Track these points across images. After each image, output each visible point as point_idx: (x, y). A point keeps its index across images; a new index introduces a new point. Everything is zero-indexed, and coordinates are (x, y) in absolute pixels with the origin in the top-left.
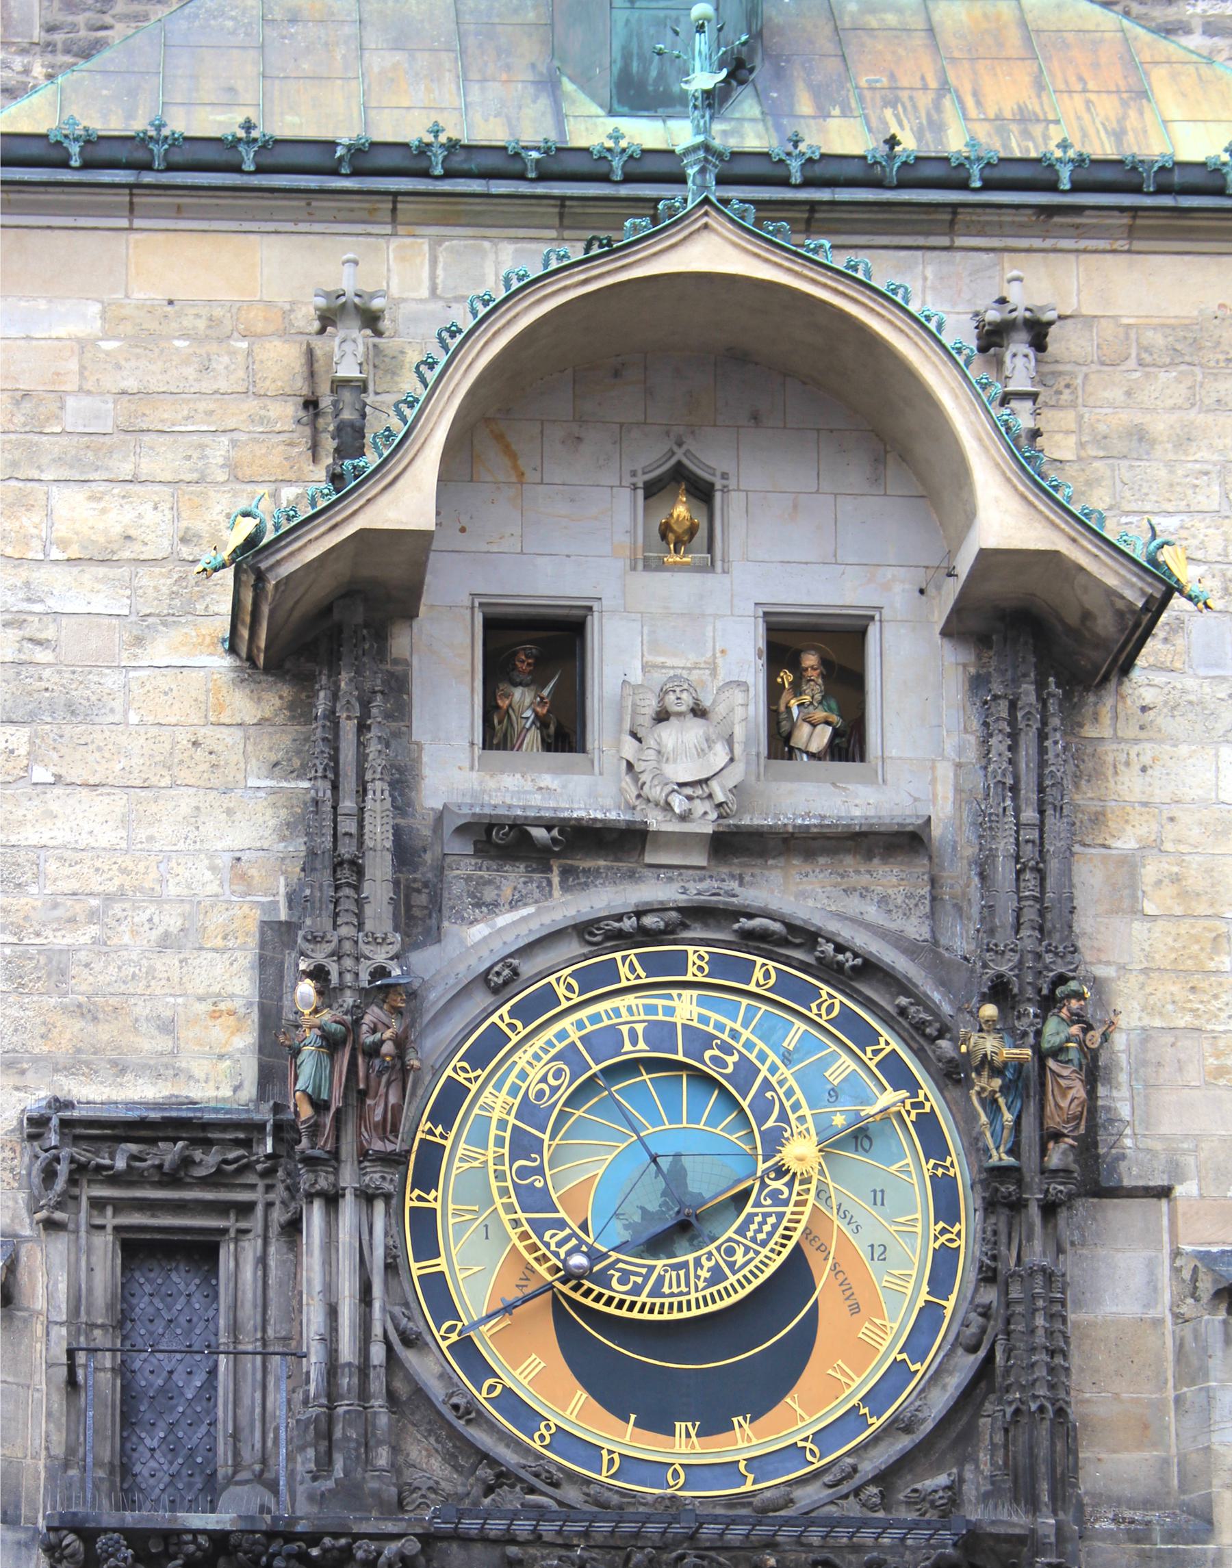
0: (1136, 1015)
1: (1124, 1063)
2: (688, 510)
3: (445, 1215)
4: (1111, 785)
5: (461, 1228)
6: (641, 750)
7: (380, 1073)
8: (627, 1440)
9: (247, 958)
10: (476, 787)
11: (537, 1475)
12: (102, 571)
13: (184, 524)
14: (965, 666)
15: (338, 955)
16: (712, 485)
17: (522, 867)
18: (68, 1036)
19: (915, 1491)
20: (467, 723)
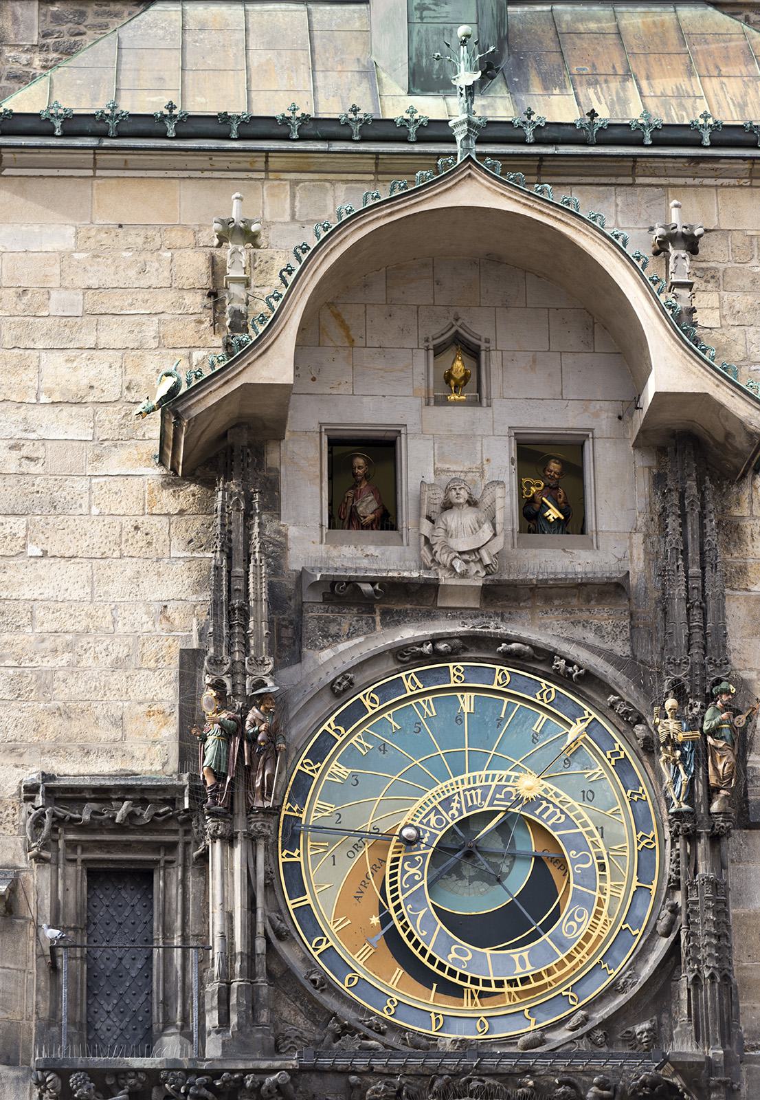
2: (463, 364)
6: (434, 529)
7: (260, 753)
8: (431, 1002)
10: (325, 555)
11: (370, 1027)
13: (128, 377)
14: (650, 468)
15: (232, 673)
16: (479, 346)
18: (51, 730)
19: (629, 1032)
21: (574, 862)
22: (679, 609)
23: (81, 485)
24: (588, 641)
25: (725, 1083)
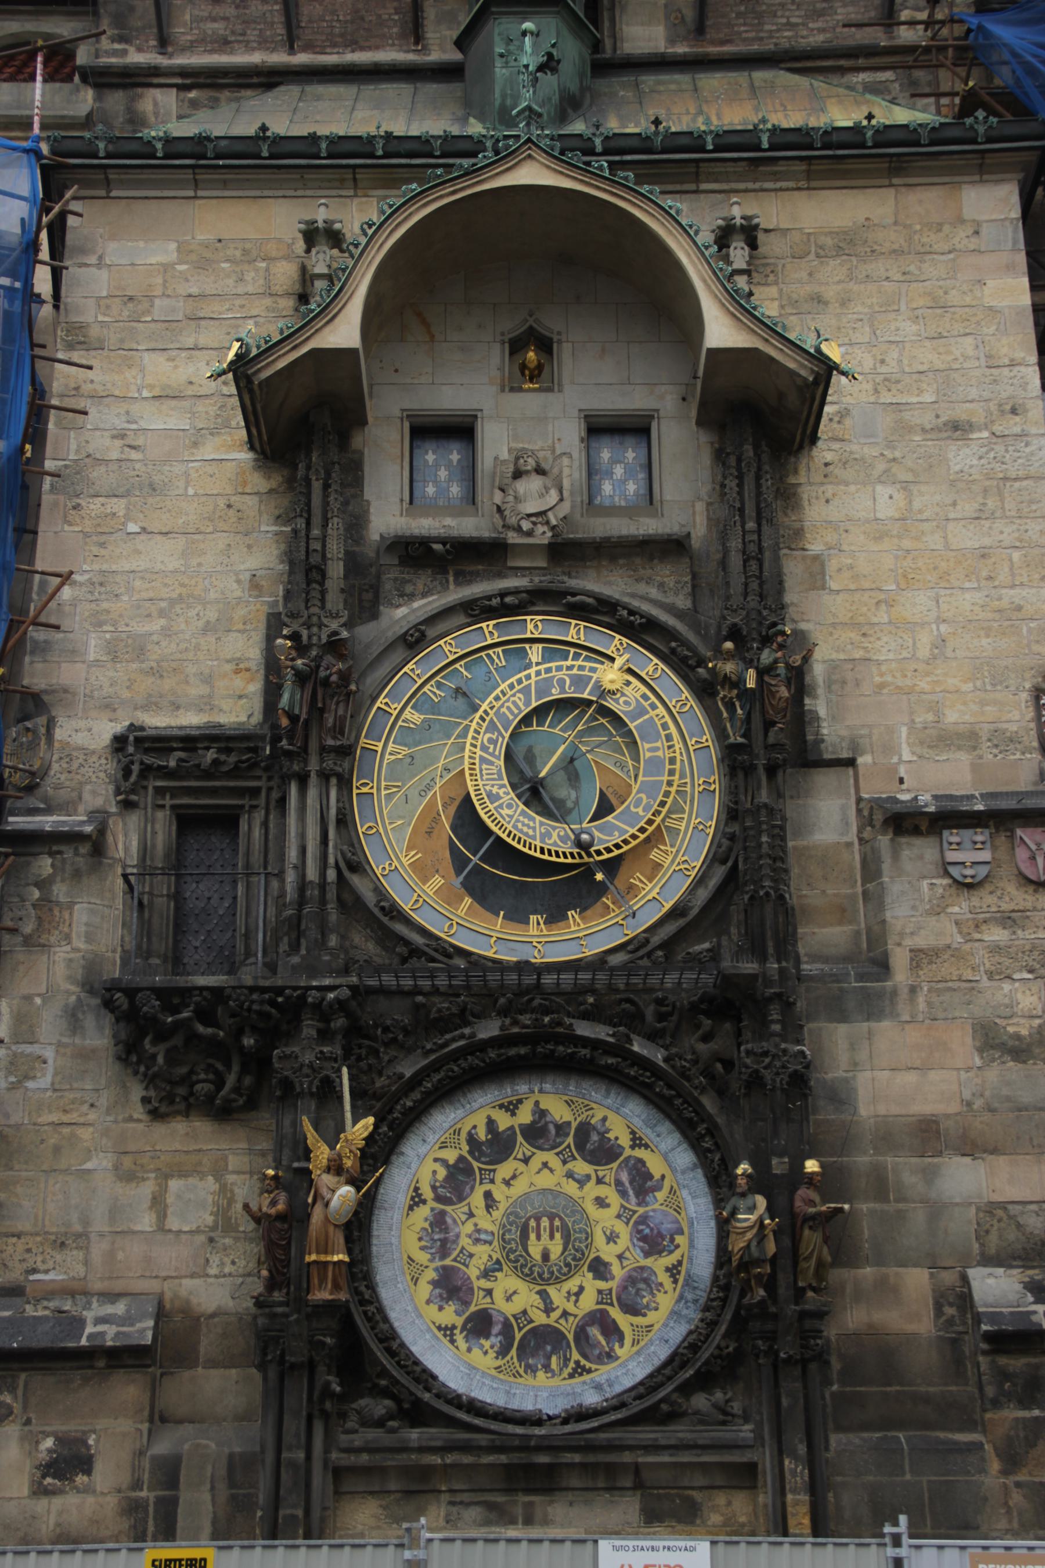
4: (807, 511)
5: (389, 797)
8: (498, 928)
9: (258, 637)
11: (436, 950)
14: (712, 443)
17: (430, 572)
20: (399, 488)
21: (563, 690)
23: (178, 469)
25: (779, 996)
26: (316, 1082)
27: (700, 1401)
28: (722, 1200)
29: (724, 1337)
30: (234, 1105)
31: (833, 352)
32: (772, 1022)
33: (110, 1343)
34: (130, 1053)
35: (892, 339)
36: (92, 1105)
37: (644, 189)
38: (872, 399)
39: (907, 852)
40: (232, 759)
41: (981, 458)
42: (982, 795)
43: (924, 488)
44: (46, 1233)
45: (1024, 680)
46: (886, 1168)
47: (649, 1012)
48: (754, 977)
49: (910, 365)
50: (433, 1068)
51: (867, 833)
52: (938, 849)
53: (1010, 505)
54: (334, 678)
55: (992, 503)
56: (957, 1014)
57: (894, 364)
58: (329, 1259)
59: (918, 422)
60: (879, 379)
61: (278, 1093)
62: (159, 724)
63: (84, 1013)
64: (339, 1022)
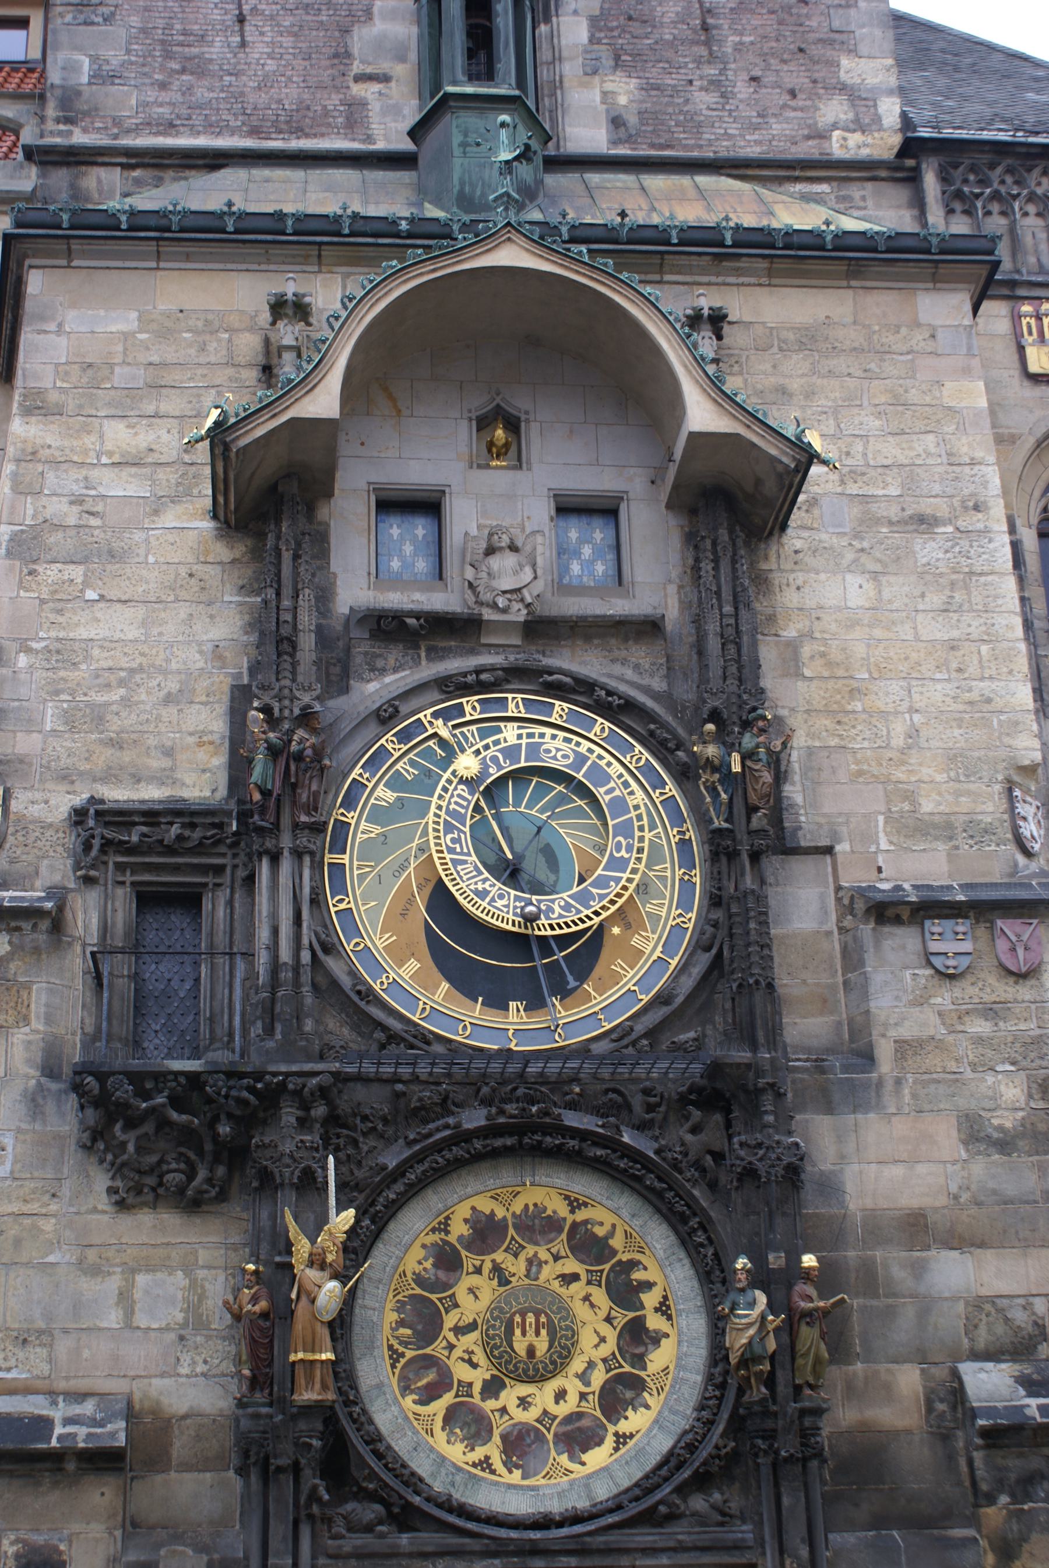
0: (803, 739)
1: (797, 770)
3: (351, 869)
5: (362, 877)
7: (306, 771)
8: (477, 1014)
9: (222, 707)
11: (415, 1037)
12: (133, 470)
14: (682, 527)
22: (713, 644)
23: (138, 536)
24: (627, 677)
25: (772, 1085)
26: (297, 1173)
27: (698, 1503)
28: (716, 1296)
29: (722, 1436)
30: (206, 1196)
31: (814, 439)
32: (766, 1112)
33: (81, 1445)
34: (96, 1140)
35: (856, 432)
36: (54, 1195)
37: (624, 276)
38: (839, 490)
39: (889, 942)
40: (197, 834)
41: (947, 552)
42: (960, 886)
43: (892, 579)
44: (7, 1329)
45: (997, 772)
46: (874, 1262)
47: (637, 1102)
48: (748, 1066)
49: (875, 459)
50: (418, 1158)
51: (848, 921)
52: (920, 939)
53: (977, 598)
54: (309, 752)
55: (958, 596)
56: (942, 1106)
57: (859, 457)
58: (317, 1357)
59: (885, 514)
60: (845, 470)
61: (255, 1184)
62: (120, 798)
63: (44, 1098)
64: (320, 1111)
